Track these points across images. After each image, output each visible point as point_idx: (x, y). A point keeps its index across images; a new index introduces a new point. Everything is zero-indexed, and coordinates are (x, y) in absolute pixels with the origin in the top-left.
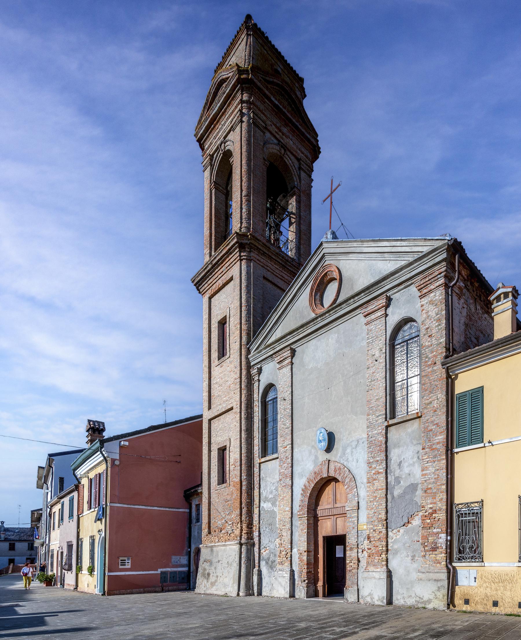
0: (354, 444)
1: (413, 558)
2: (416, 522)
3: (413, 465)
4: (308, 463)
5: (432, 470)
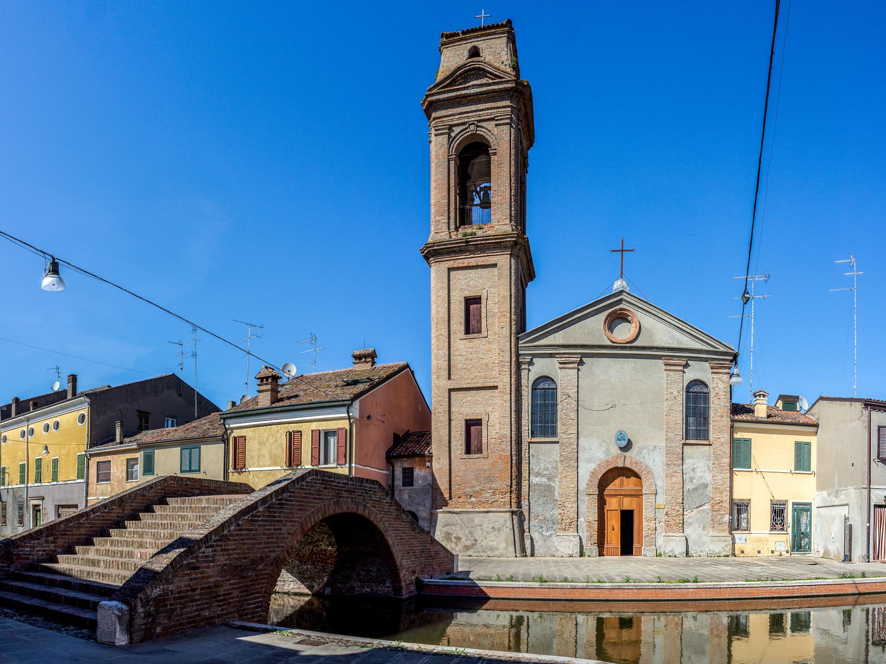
0: (651, 448)
1: (704, 528)
2: (707, 507)
3: (705, 472)
4: (597, 454)
5: (720, 477)
